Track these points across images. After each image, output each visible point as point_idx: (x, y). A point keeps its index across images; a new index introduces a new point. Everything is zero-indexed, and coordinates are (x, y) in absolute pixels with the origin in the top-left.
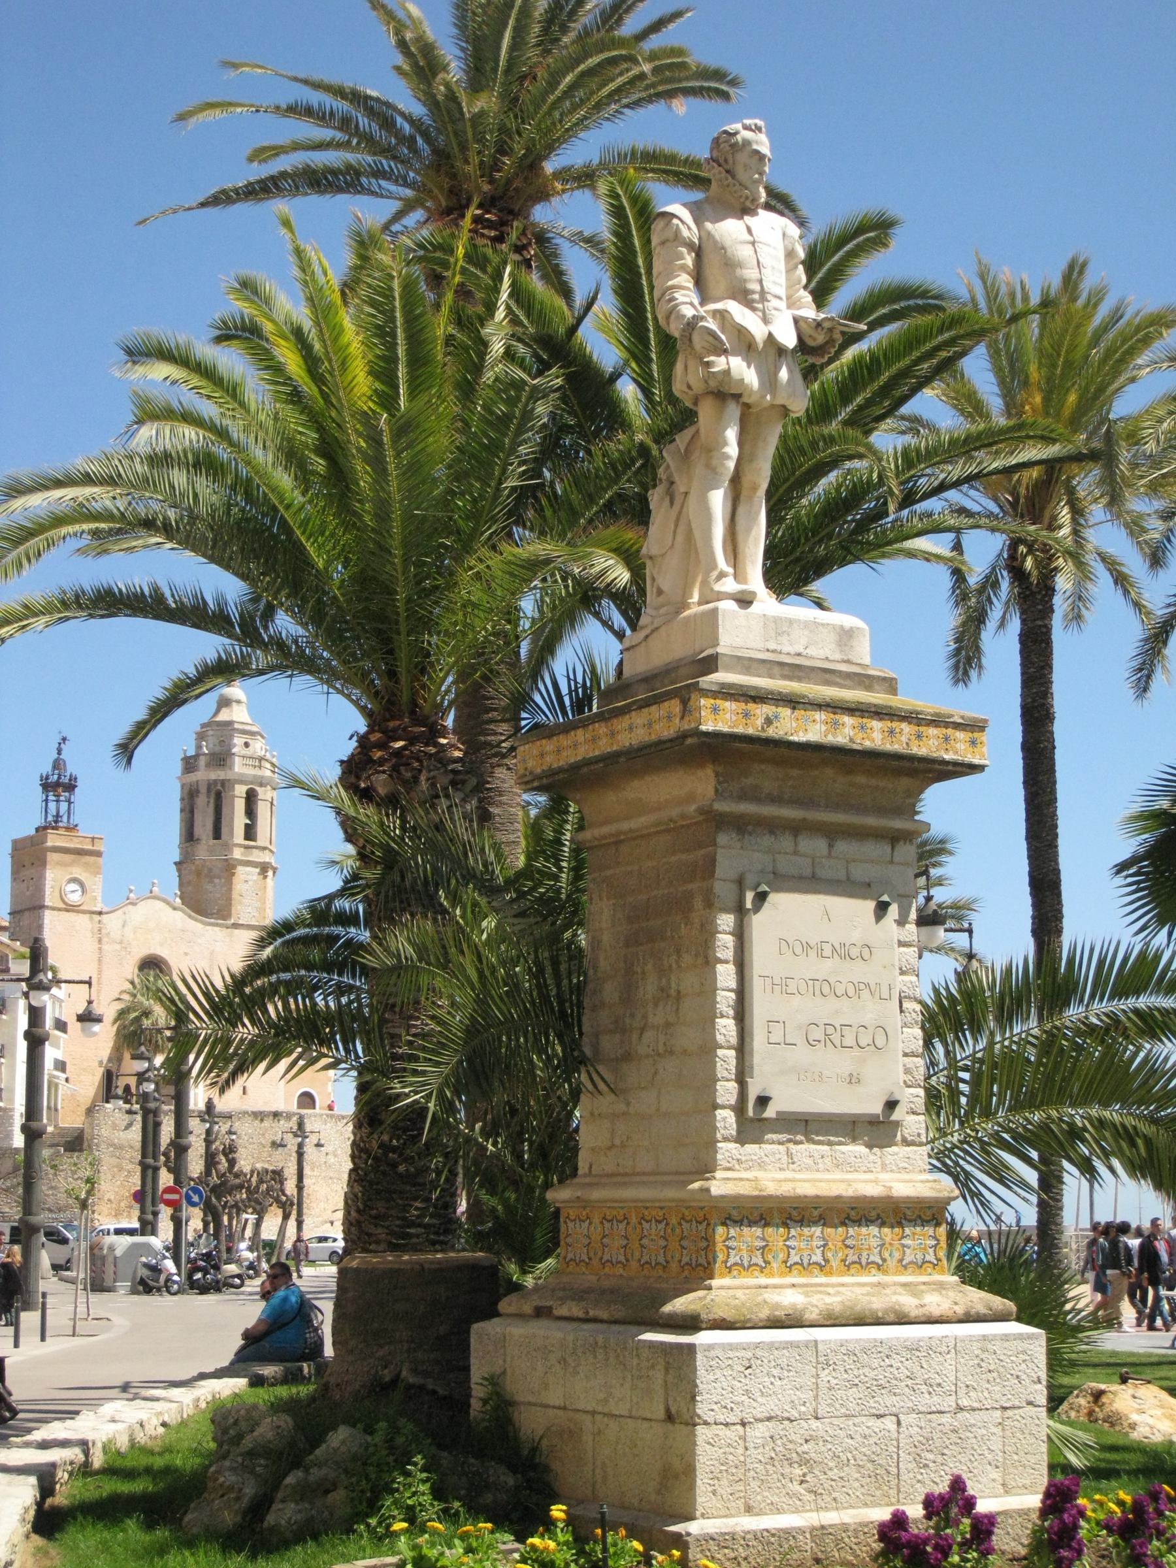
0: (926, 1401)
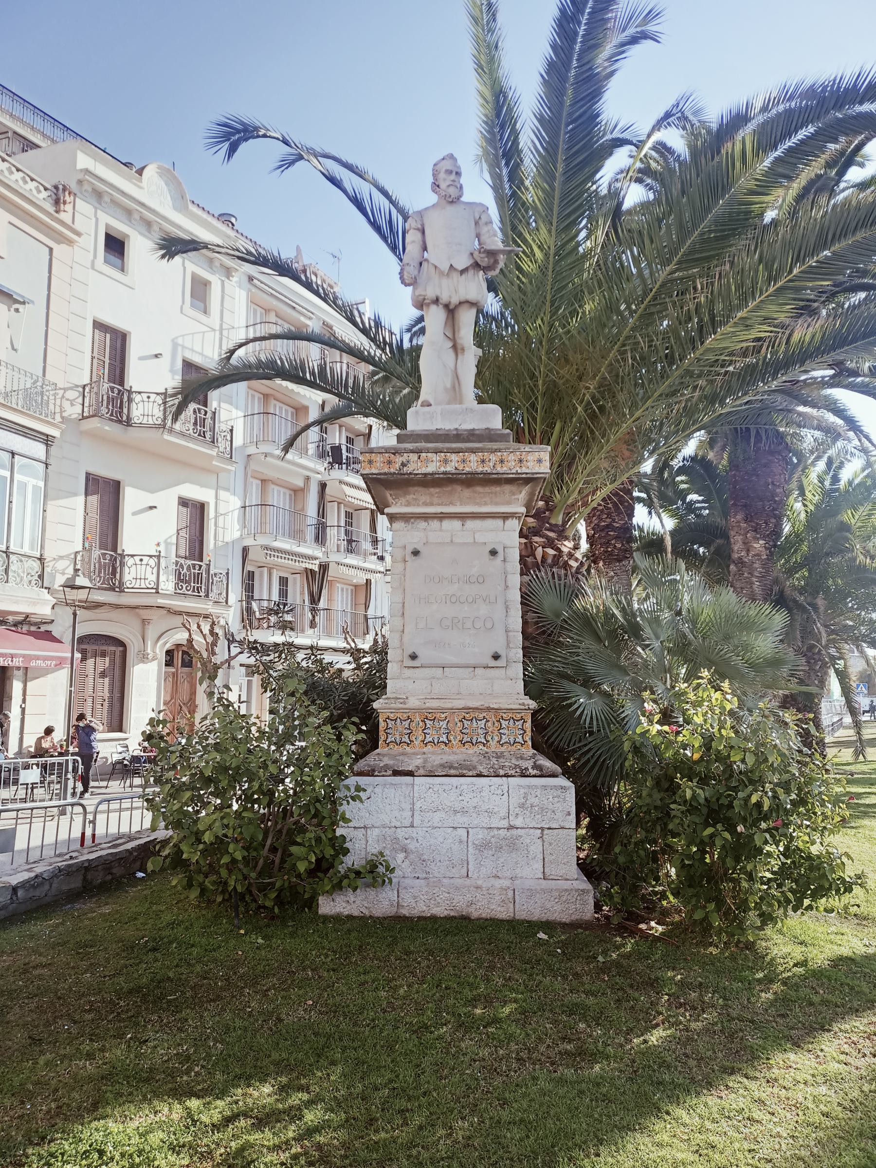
0: (485, 821)
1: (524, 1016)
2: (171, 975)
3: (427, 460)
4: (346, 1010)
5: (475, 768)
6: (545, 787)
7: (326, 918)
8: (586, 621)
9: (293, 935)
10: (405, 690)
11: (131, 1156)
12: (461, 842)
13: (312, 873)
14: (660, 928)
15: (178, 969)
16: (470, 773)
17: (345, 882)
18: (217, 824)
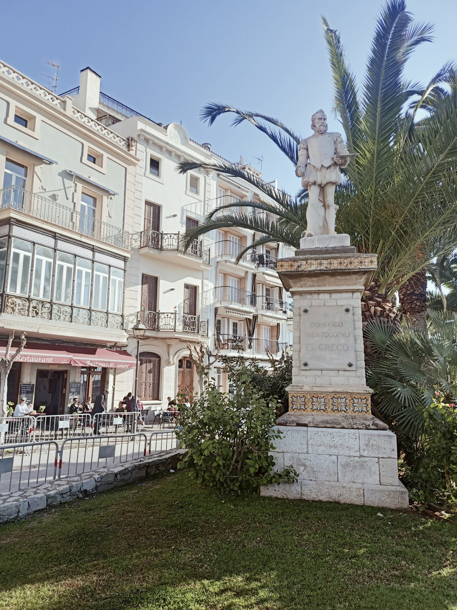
1: (371, 555)
2: (190, 520)
3: (311, 264)
4: (277, 544)
5: (340, 424)
6: (379, 435)
7: (264, 498)
8: (400, 346)
9: (248, 505)
10: (301, 382)
11: (178, 603)
12: (334, 463)
13: (257, 474)
14: (448, 515)
15: (194, 517)
16: (338, 427)
17: (274, 480)
18: (211, 446)
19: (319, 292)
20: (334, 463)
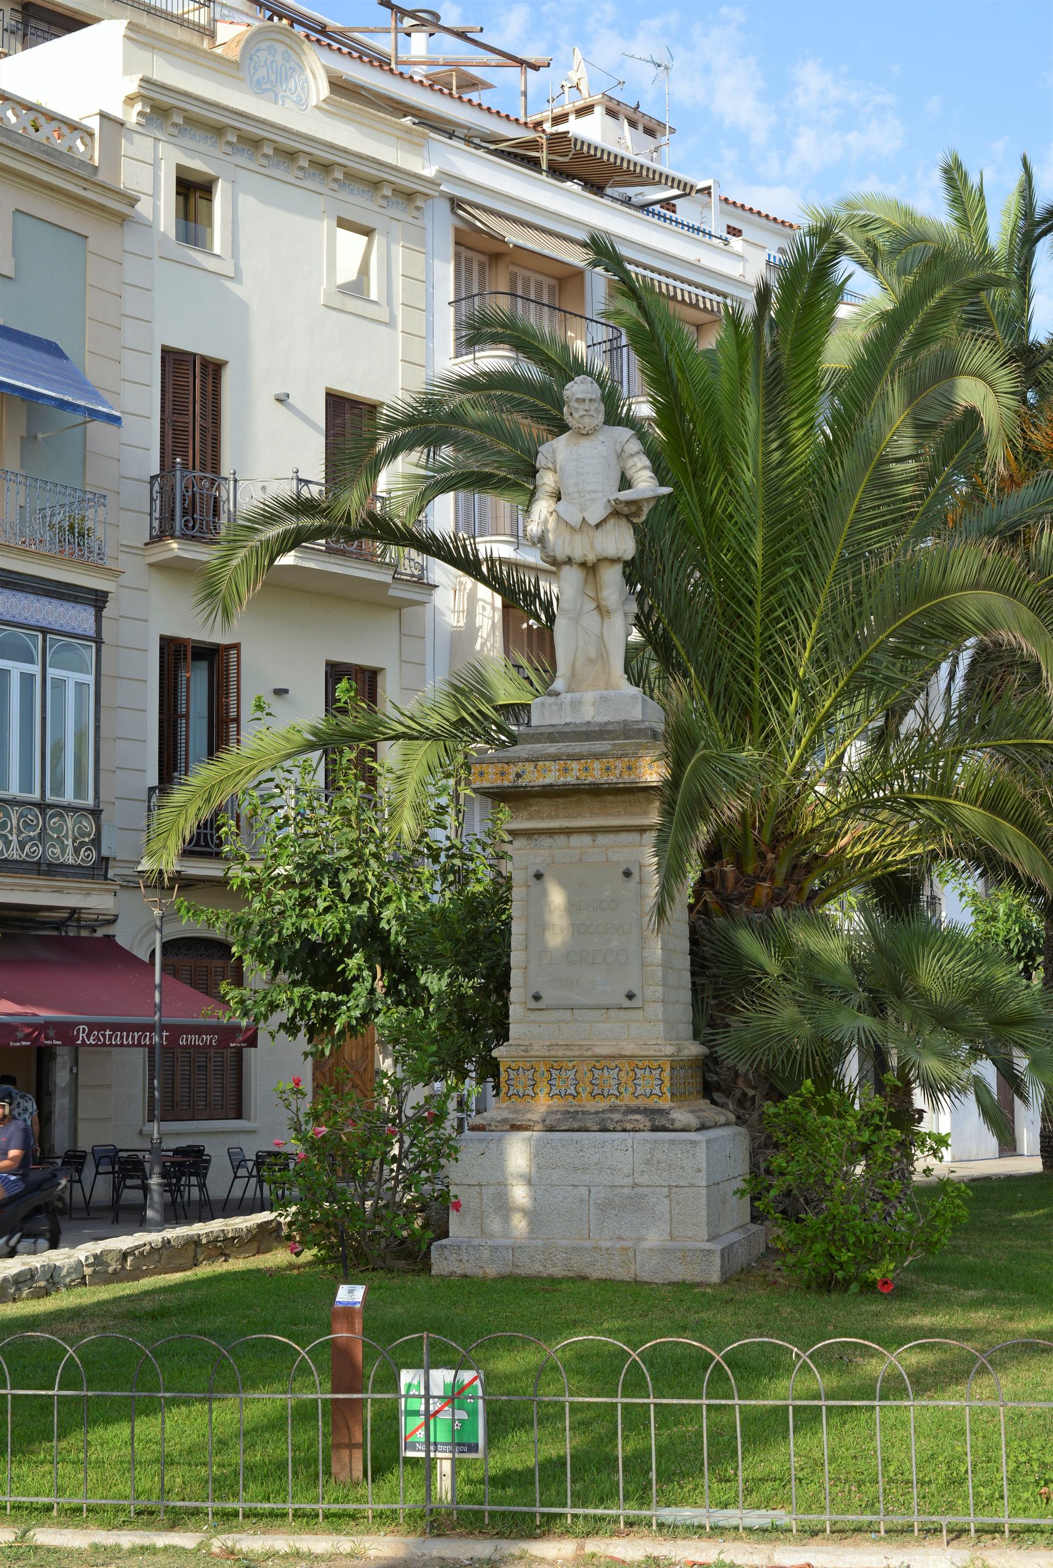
3: (546, 770)
6: (672, 1142)
19: (569, 832)
20: (582, 1201)
